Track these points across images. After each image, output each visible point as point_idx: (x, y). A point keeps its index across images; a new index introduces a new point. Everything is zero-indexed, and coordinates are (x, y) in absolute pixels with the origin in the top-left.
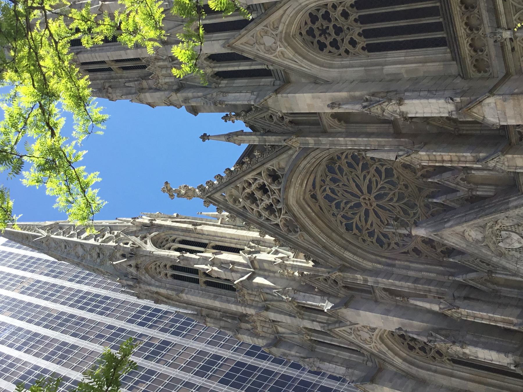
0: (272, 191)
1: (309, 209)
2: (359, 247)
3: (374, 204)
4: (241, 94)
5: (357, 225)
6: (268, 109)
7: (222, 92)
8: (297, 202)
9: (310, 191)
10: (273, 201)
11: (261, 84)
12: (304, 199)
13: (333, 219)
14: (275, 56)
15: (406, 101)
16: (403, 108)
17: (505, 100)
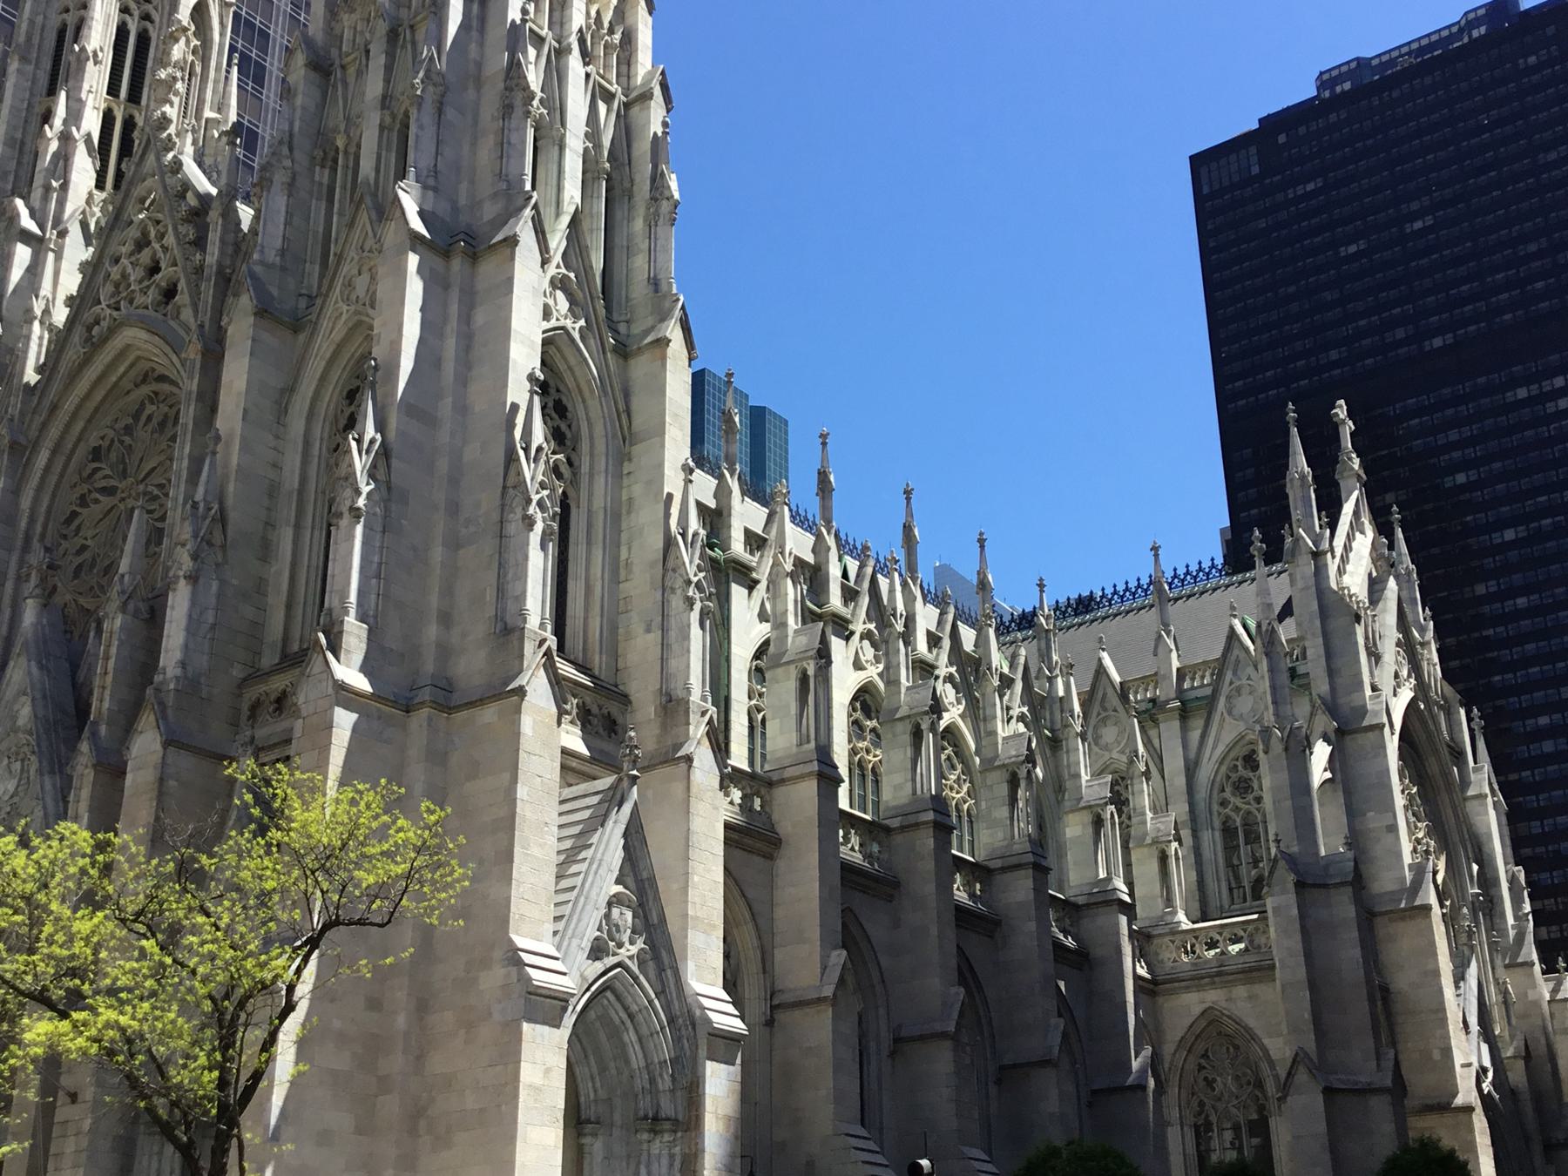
0: (148, 287)
1: (122, 369)
2: (62, 476)
3: (122, 506)
4: (282, 227)
5: (100, 469)
6: (236, 295)
7: (294, 178)
8: (128, 346)
9: (153, 370)
10: (133, 291)
11: (307, 265)
12: (139, 358)
13: (108, 420)
14: (336, 302)
15: (189, 588)
16: (182, 582)
17: (155, 768)
